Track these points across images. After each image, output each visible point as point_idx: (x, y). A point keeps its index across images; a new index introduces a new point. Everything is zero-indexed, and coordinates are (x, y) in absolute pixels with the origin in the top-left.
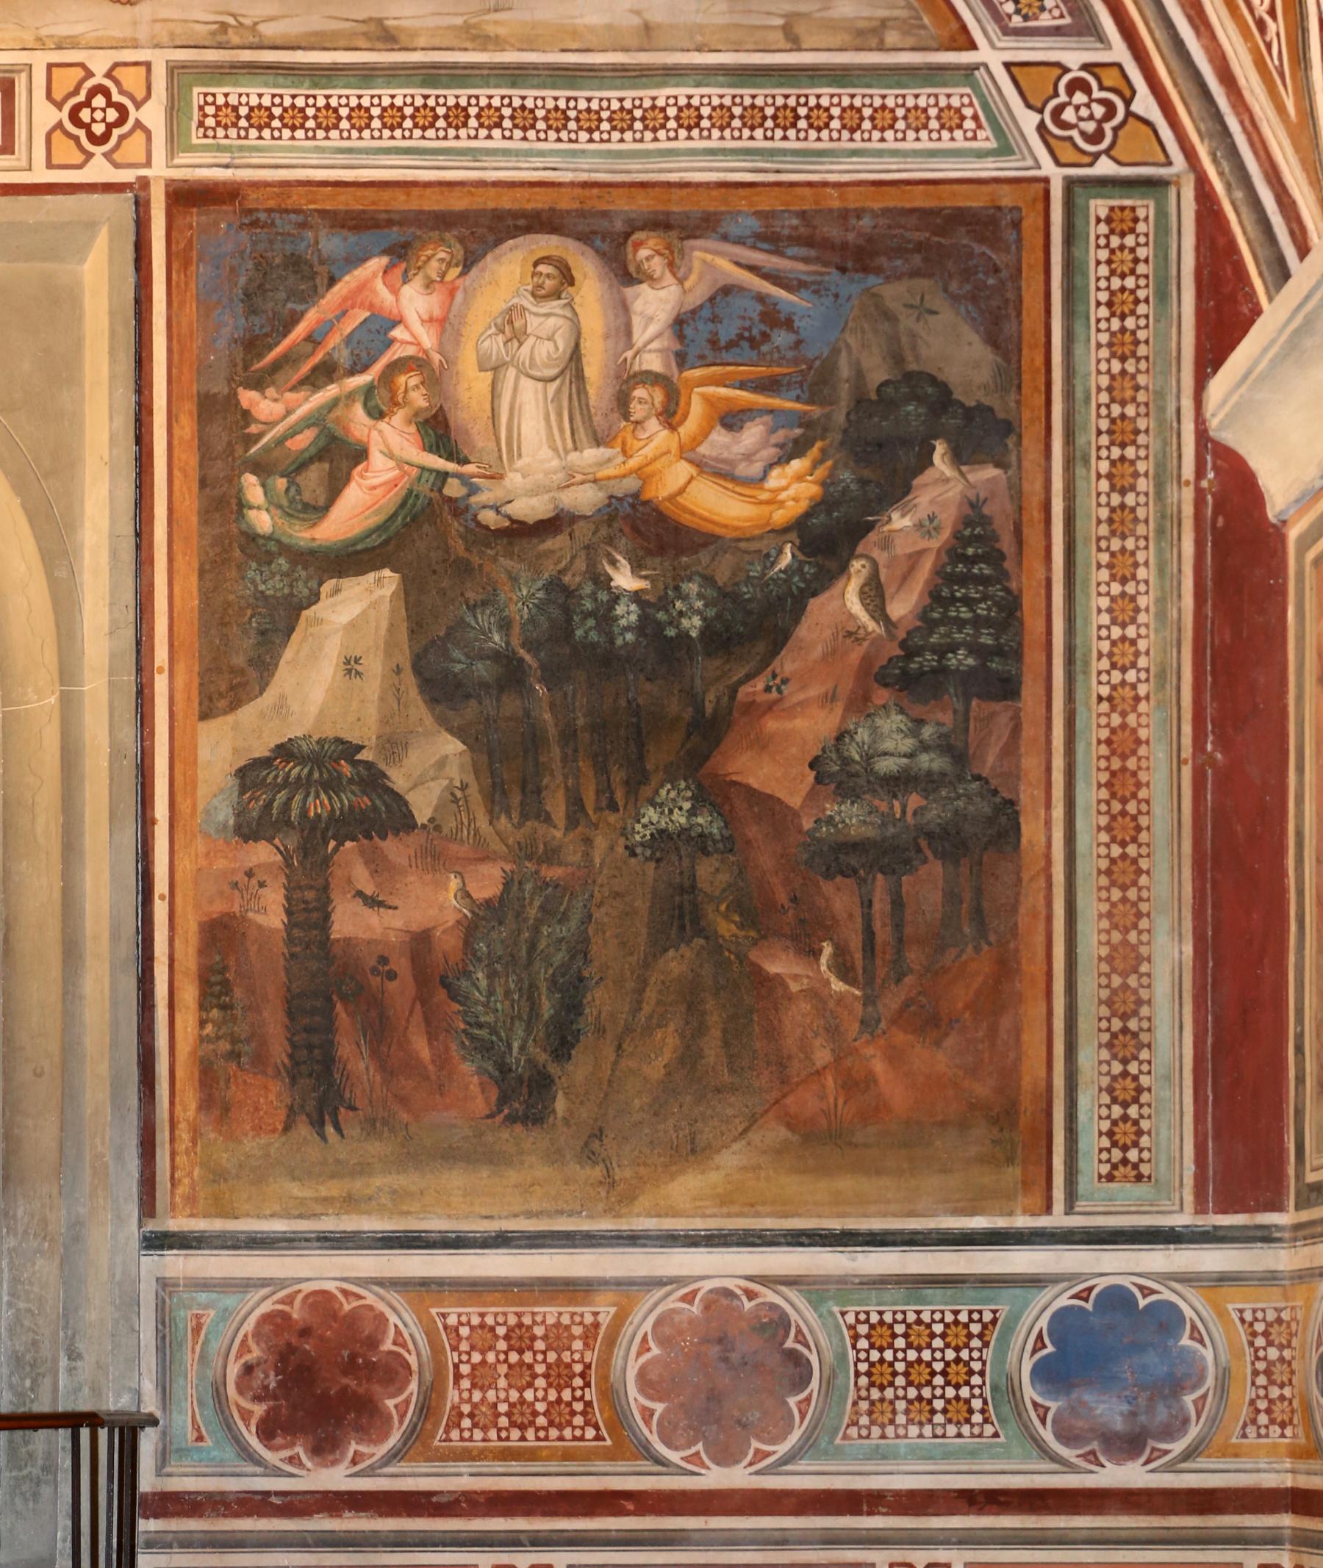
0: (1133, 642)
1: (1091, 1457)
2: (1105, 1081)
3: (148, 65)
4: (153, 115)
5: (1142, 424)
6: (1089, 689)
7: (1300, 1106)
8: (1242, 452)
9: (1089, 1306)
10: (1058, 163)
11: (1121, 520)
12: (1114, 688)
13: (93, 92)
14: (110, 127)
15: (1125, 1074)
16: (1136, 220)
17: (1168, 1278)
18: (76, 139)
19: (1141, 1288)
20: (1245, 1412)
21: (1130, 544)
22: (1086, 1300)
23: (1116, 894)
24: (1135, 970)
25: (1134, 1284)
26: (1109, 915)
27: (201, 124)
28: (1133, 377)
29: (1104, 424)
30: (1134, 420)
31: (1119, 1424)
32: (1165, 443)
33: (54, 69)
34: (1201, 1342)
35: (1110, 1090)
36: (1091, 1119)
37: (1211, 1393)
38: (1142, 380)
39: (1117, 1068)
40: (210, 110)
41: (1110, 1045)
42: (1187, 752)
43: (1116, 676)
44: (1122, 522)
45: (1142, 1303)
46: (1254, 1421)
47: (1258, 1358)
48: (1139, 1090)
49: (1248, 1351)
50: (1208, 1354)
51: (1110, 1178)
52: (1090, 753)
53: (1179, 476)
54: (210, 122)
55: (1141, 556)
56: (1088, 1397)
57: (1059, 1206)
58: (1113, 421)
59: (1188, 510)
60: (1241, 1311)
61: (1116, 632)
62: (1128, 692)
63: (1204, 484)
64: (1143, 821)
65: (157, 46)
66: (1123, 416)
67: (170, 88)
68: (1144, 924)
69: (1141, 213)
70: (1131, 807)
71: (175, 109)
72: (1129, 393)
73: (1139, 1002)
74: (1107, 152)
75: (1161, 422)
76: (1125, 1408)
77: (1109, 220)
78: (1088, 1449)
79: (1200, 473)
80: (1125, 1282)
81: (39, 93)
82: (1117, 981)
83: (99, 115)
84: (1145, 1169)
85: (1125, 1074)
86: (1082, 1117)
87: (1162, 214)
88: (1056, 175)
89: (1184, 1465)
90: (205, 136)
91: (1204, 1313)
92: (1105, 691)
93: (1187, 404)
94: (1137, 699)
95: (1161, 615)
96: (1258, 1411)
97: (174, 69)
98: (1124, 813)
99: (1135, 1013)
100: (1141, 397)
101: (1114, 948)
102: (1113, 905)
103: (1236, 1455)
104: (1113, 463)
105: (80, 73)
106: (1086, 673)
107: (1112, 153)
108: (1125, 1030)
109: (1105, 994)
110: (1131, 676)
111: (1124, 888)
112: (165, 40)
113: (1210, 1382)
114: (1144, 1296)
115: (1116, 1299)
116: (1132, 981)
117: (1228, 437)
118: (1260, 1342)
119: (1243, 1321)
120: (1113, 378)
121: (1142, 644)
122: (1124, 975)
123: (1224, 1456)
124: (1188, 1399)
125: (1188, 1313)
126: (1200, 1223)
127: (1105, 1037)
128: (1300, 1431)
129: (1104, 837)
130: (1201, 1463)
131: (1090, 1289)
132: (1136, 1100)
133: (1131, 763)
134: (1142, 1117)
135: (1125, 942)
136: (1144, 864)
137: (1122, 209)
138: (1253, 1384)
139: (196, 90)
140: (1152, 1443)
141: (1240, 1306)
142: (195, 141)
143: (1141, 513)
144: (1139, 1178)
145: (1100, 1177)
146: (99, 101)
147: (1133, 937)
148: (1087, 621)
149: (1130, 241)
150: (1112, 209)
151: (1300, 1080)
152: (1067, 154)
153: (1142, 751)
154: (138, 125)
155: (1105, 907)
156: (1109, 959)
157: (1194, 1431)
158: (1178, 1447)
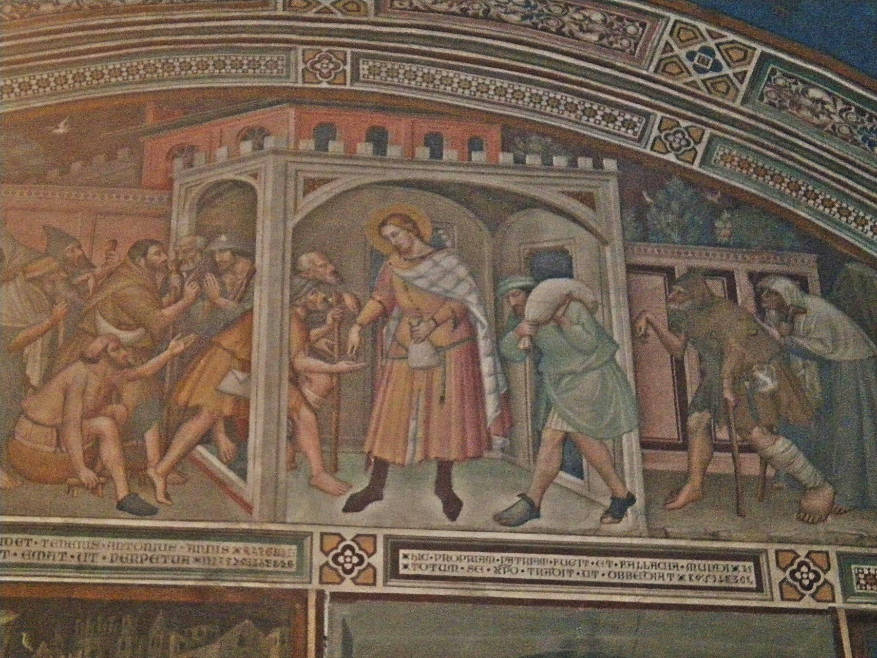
3: (827, 553)
4: (833, 576)
13: (801, 564)
14: (811, 582)
18: (795, 587)
27: (858, 583)
33: (780, 553)
40: (862, 576)
54: (863, 582)
65: (829, 544)
67: (840, 565)
71: (844, 574)
81: (773, 564)
83: (805, 576)
90: (861, 589)
97: (839, 555)
105: (792, 555)
112: (833, 540)
139: (853, 566)
142: (857, 591)
146: (804, 569)
154: (826, 581)
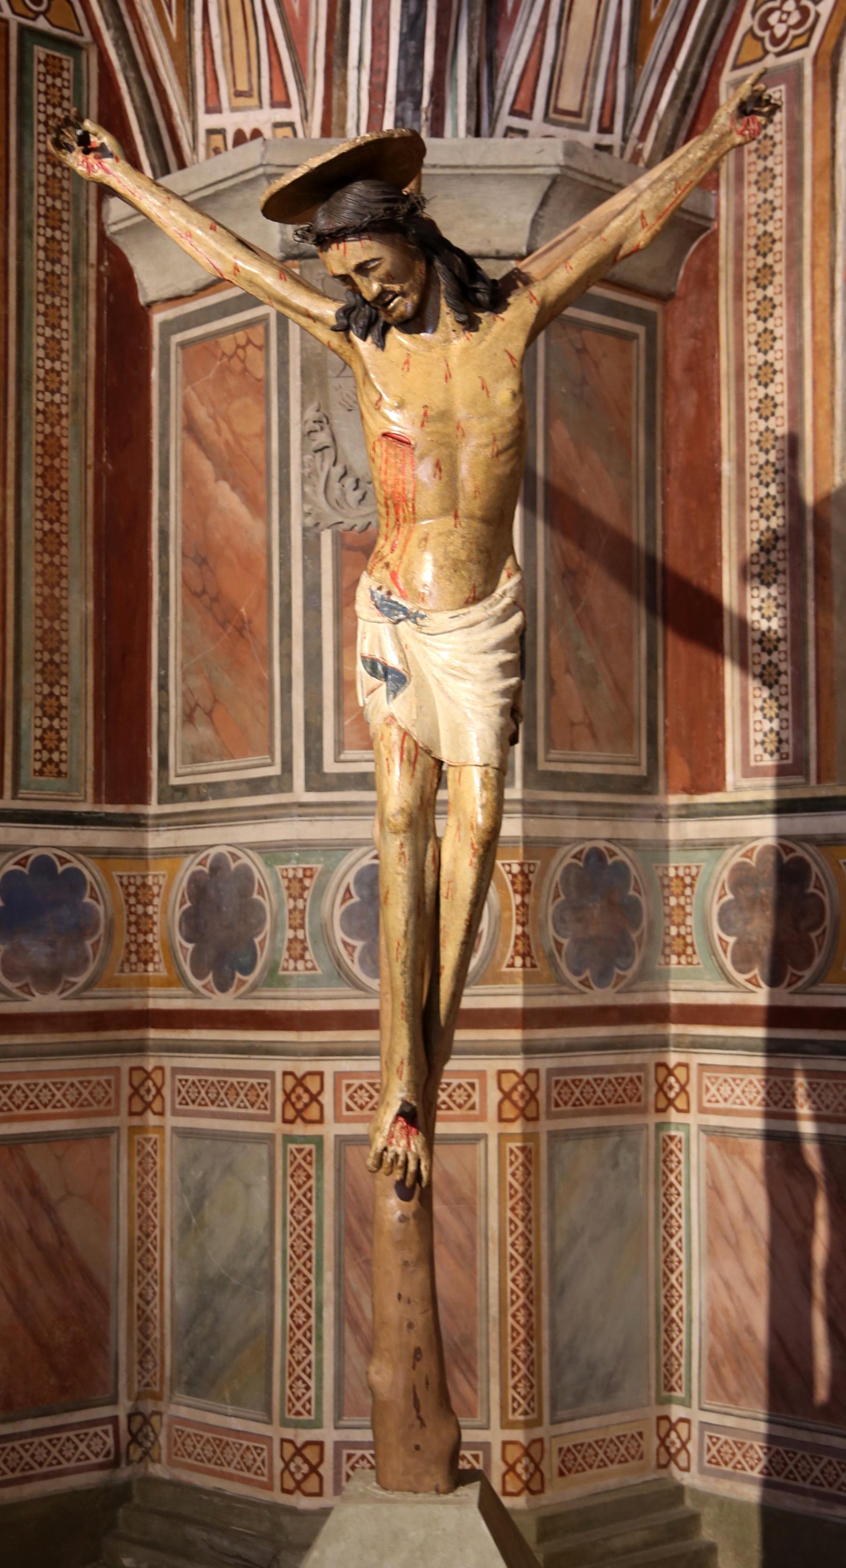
0: (59, 374)
1: (25, 989)
2: (39, 699)
5: (65, 216)
6: (30, 402)
7: (163, 728)
8: (126, 251)
9: (26, 871)
10: (14, 12)
11: (52, 282)
12: (46, 405)
15: (51, 694)
16: (62, 68)
17: (76, 851)
19: (60, 858)
20: (123, 952)
21: (57, 301)
22: (24, 866)
23: (47, 559)
24: (58, 617)
25: (56, 855)
26: (42, 574)
28: (60, 181)
29: (42, 210)
30: (60, 212)
31: (44, 962)
32: (79, 234)
34: (97, 900)
35: (42, 706)
36: (30, 726)
37: (102, 939)
38: (65, 184)
39: (46, 689)
41: (42, 672)
42: (91, 461)
43: (48, 397)
44: (53, 285)
45: (60, 869)
46: (128, 960)
47: (131, 913)
48: (60, 707)
49: (125, 907)
50: (101, 909)
51: (41, 773)
52: (32, 450)
53: (87, 259)
55: (64, 312)
56: (24, 942)
57: (8, 793)
58: (47, 209)
59: (92, 285)
60: (121, 877)
61: (48, 364)
62: (54, 409)
63: (102, 269)
64: (64, 506)
66: (54, 208)
68: (64, 583)
69: (65, 64)
70: (57, 495)
72: (57, 192)
73: (61, 642)
74: (44, 13)
75: (77, 218)
76: (48, 950)
77: (46, 63)
78: (24, 982)
79: (100, 261)
80: (49, 852)
82: (47, 624)
84: (63, 767)
85: (51, 694)
86: (24, 725)
87: (78, 69)
88: (15, 21)
89: (86, 994)
91: (99, 878)
92: (41, 406)
93: (92, 208)
94: (61, 416)
95: (76, 357)
96: (130, 952)
98: (52, 499)
99: (58, 649)
100: (65, 196)
101: (45, 599)
102: (45, 566)
103: (118, 986)
104: (47, 240)
106: (30, 390)
107: (48, 15)
108: (52, 662)
109: (39, 633)
110: (57, 398)
111: (52, 555)
113: (102, 930)
114: (62, 864)
115: (44, 865)
116: (57, 625)
117: (120, 241)
118: (132, 901)
119: (122, 884)
120: (48, 177)
121: (64, 376)
122: (52, 619)
123: (110, 986)
124: (89, 943)
125: (89, 877)
126: (97, 810)
127: (39, 665)
128: (162, 967)
129: (39, 515)
130: (96, 992)
131: (27, 858)
132: (58, 715)
133: (57, 463)
134: (62, 728)
135: (52, 596)
136: (64, 538)
137: (54, 57)
138: (128, 932)
140: (65, 977)
141: (120, 873)
143: (64, 280)
144: (60, 774)
145: (35, 771)
147: (57, 592)
148: (30, 353)
149: (58, 82)
150: (48, 56)
151: (164, 709)
152: (20, 9)
153: (64, 455)
155: (39, 567)
156: (42, 607)
157: (92, 968)
158: (81, 980)
